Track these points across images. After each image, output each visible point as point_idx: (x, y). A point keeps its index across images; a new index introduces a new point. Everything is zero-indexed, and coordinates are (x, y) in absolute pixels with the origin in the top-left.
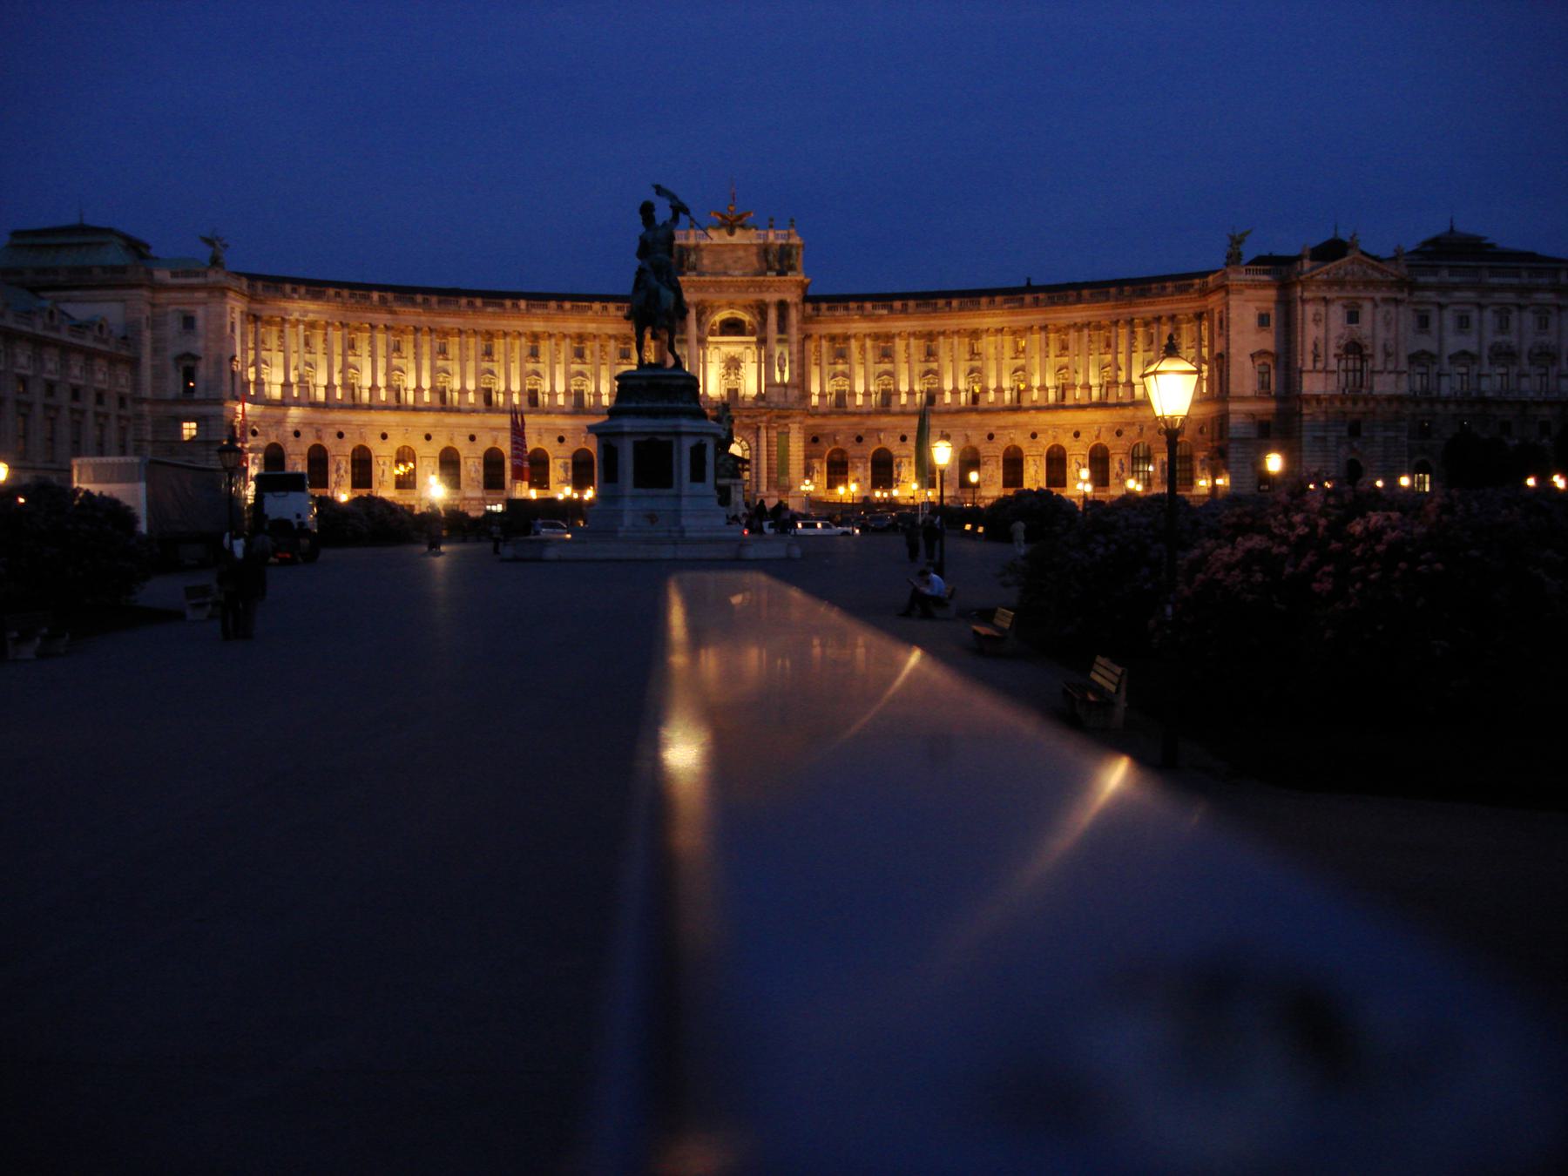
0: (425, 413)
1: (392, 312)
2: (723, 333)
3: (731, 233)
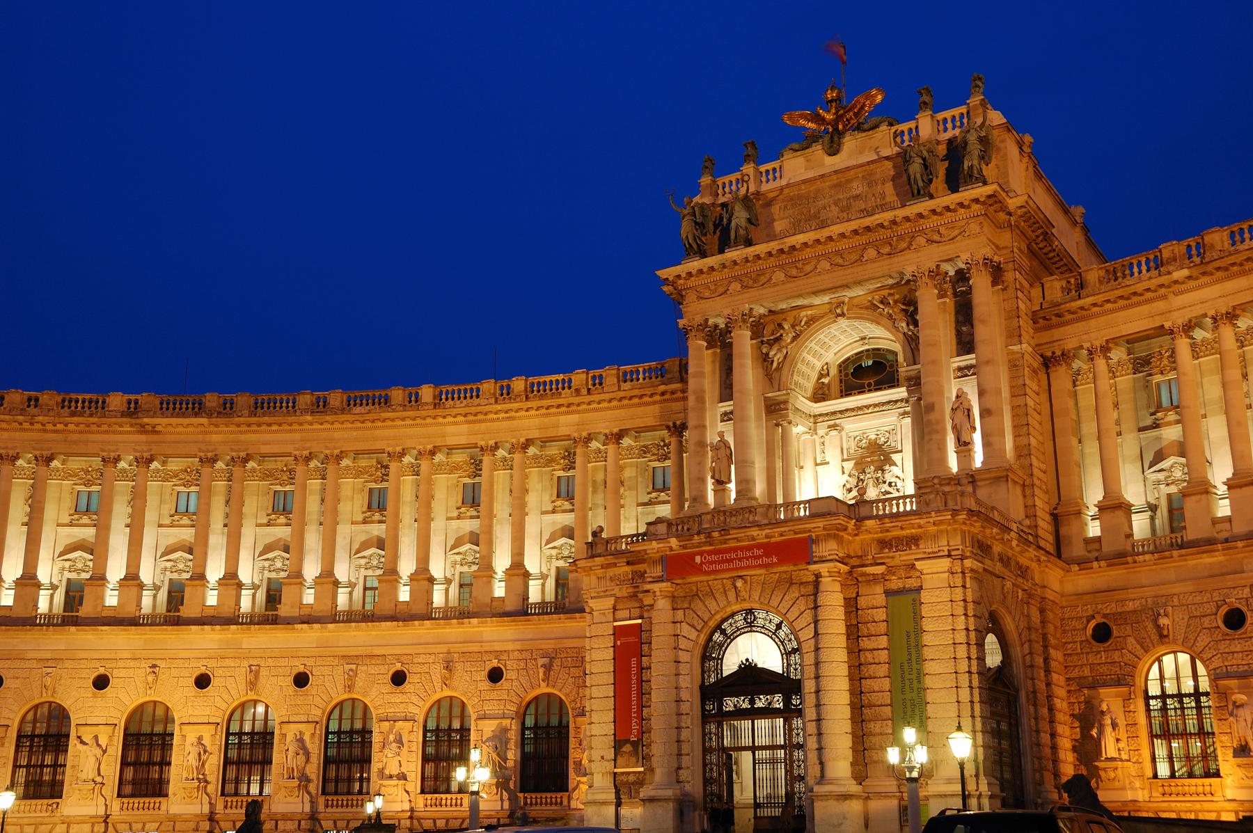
0: (193, 627)
1: (143, 430)
2: (847, 391)
3: (833, 150)
